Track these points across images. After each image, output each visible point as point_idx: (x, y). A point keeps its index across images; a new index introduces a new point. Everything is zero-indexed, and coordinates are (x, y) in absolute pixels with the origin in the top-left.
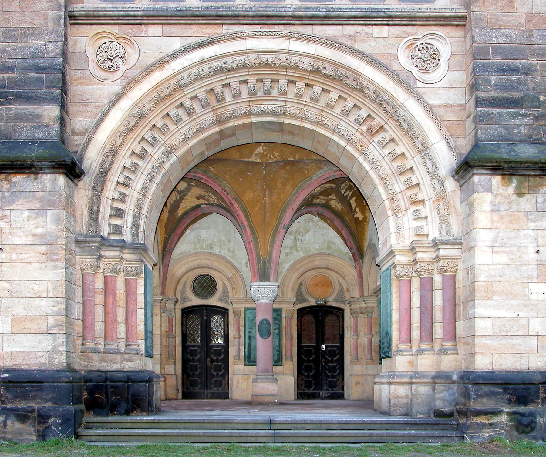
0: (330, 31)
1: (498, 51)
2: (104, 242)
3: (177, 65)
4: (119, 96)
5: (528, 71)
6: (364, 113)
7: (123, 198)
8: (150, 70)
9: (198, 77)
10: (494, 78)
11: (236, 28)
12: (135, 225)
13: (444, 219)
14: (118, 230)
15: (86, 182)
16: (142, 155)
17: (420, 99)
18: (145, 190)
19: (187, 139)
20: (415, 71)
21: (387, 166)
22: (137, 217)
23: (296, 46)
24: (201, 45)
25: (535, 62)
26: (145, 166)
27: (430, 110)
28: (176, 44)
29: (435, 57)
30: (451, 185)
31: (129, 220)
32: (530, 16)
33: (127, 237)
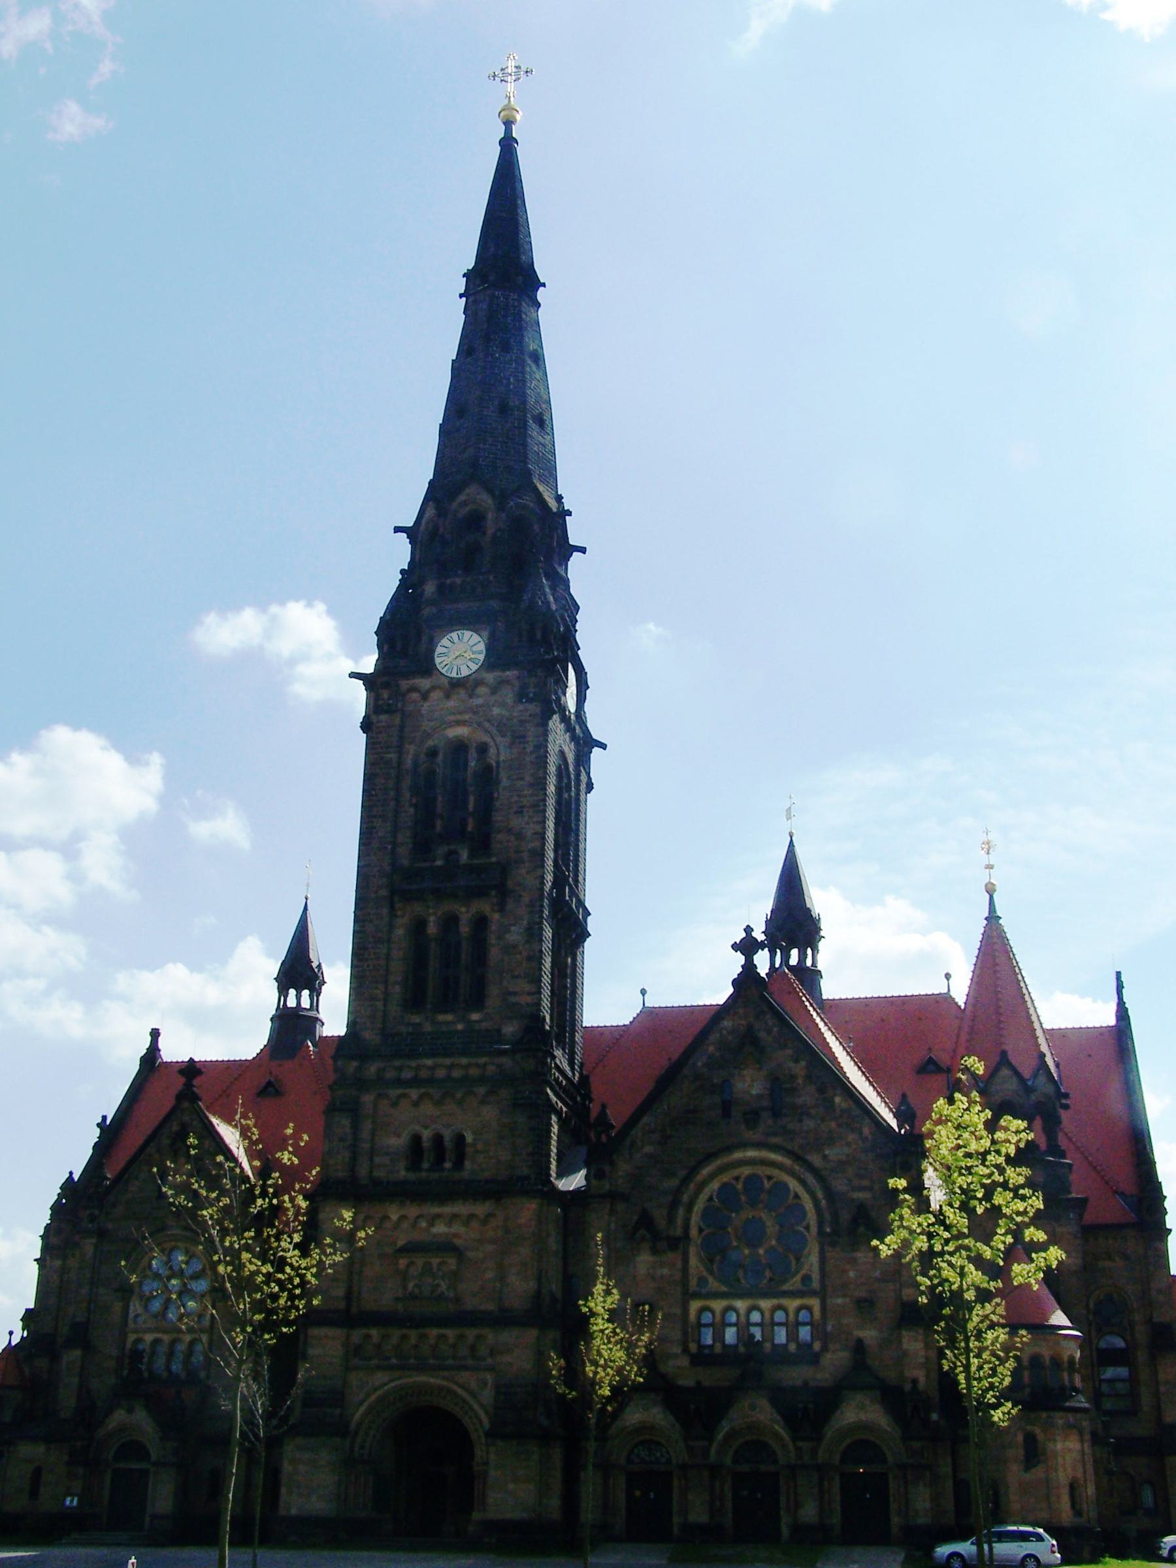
0: (446, 1373)
8: (376, 1389)
23: (432, 1380)
29: (486, 1384)
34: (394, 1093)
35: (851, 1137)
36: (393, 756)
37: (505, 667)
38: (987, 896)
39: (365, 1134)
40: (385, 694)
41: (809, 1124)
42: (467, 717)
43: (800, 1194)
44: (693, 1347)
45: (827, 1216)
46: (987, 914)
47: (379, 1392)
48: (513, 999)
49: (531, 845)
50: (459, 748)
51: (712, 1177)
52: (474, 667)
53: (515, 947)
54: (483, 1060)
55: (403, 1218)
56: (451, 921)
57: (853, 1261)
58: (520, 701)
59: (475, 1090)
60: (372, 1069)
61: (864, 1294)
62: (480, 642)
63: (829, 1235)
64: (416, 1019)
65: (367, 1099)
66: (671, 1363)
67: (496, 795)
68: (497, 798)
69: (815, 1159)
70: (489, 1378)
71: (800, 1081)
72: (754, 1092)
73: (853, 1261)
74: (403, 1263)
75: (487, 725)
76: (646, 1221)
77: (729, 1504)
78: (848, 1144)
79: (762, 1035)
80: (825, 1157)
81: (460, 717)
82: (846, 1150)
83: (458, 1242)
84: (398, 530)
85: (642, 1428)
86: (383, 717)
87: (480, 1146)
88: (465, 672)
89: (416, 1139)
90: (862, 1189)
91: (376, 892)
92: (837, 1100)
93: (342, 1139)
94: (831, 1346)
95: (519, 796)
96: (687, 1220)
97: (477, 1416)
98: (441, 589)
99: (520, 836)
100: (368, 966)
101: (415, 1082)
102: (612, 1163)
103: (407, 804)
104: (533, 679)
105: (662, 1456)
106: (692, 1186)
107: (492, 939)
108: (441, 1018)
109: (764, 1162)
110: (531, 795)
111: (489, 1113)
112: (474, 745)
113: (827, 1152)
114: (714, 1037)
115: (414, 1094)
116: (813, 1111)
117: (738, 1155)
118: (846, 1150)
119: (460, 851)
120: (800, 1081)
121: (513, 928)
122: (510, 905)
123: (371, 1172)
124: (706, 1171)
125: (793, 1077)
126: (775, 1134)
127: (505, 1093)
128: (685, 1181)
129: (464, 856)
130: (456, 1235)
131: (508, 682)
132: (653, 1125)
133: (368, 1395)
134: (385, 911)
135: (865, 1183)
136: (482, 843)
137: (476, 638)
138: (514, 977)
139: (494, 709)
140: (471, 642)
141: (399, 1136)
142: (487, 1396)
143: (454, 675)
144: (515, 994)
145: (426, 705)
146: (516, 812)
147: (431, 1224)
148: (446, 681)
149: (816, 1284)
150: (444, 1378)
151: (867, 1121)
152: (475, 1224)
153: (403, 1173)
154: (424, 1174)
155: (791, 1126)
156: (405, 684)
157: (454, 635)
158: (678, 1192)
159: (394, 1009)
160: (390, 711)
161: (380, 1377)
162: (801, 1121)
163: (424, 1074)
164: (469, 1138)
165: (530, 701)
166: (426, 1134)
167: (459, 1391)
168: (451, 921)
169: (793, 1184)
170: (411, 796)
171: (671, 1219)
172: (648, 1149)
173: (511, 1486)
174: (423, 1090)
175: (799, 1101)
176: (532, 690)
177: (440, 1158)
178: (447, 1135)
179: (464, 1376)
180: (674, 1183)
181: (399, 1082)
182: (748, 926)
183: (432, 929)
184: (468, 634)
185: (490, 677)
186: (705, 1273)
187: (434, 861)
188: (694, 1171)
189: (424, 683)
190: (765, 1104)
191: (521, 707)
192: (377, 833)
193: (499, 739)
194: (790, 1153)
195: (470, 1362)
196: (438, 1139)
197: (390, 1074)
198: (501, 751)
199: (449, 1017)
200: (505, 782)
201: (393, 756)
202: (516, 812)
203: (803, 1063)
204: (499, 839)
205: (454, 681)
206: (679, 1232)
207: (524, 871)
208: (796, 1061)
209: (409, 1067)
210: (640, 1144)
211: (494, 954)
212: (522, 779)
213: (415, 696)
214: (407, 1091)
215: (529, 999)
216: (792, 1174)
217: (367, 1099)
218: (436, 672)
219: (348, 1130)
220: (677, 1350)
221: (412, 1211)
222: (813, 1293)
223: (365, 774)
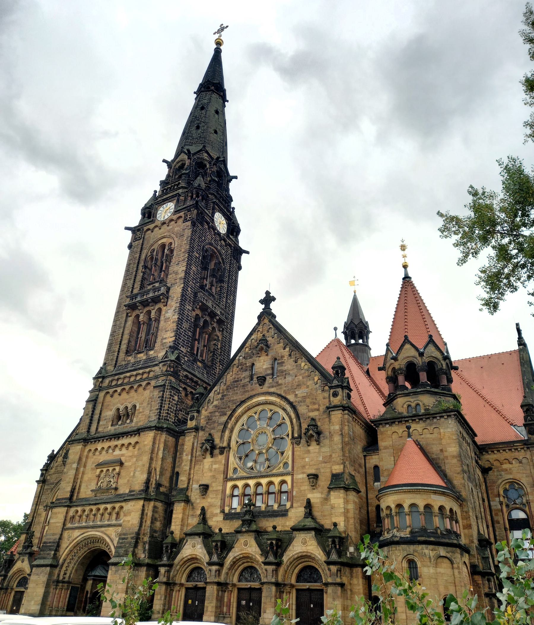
0: (103, 529)
7: (67, 570)
9: (81, 541)
11: (87, 530)
14: (64, 578)
16: (72, 559)
18: (73, 567)
24: (82, 534)
28: (79, 534)
32: (132, 524)
35: (310, 383)
41: (289, 379)
43: (285, 418)
44: (227, 510)
45: (296, 428)
55: (103, 448)
57: (309, 452)
61: (313, 471)
66: (215, 519)
69: (291, 398)
71: (286, 358)
72: (264, 367)
73: (309, 452)
76: (210, 440)
78: (308, 387)
79: (269, 339)
80: (296, 395)
82: (306, 390)
90: (313, 410)
92: (303, 364)
94: (294, 505)
106: (233, 419)
113: (297, 393)
115: (119, 389)
116: (291, 372)
117: (255, 400)
118: (306, 390)
120: (286, 358)
124: (240, 410)
125: (282, 357)
126: (273, 387)
135: (316, 406)
141: (111, 410)
144: (166, 338)
147: (114, 450)
150: (102, 532)
151: (317, 373)
152: (131, 448)
153: (110, 427)
155: (280, 382)
161: (77, 533)
162: (285, 378)
166: (121, 408)
169: (281, 412)
171: (222, 437)
172: (215, 403)
175: (285, 368)
188: (234, 411)
194: (280, 396)
203: (287, 349)
206: (225, 444)
208: (284, 349)
209: (120, 378)
220: (218, 511)
222: (287, 474)
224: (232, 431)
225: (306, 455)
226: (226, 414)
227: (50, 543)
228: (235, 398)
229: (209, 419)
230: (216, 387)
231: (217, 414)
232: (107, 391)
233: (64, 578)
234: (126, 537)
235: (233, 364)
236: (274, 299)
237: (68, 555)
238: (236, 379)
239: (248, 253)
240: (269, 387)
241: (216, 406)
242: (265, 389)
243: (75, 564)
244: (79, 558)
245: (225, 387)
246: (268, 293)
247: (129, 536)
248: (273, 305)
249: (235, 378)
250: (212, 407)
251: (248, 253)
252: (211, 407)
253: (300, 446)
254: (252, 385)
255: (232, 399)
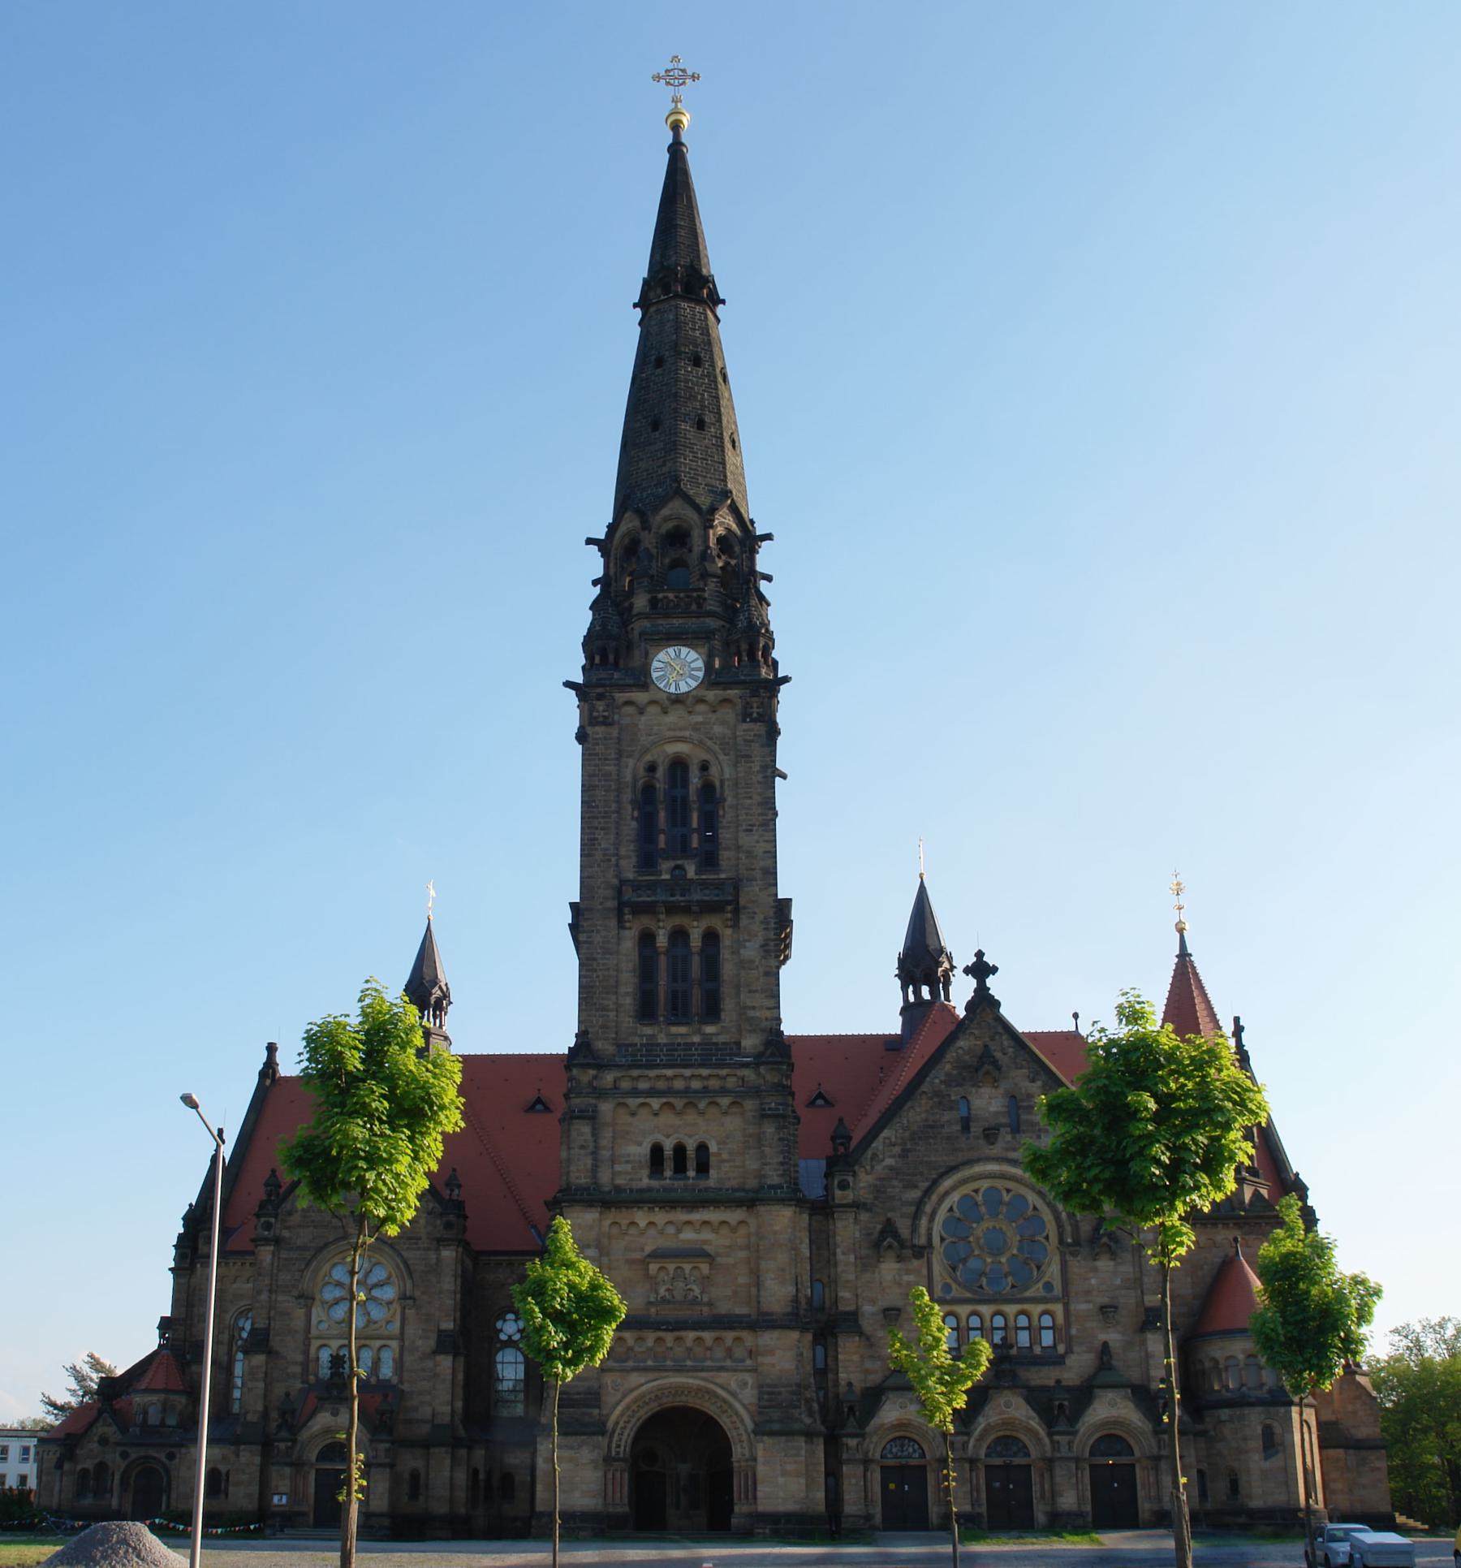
0: (704, 1374)
1: (769, 1386)
2: (615, 1460)
3: (644, 1388)
4: (621, 1401)
5: (779, 1393)
6: (719, 1405)
7: (620, 1440)
8: (633, 1390)
9: (652, 1392)
10: (766, 1397)
12: (625, 1450)
13: (751, 1450)
14: (618, 1453)
15: (608, 1434)
17: (740, 1401)
18: (629, 1435)
19: (646, 1413)
20: (738, 1391)
21: (730, 1425)
22: (625, 1447)
23: (691, 1381)
25: (782, 1389)
26: (630, 1426)
27: (744, 1405)
28: (643, 1380)
30: (752, 1436)
31: (622, 1448)
33: (622, 1455)
34: (633, 1102)
36: (612, 769)
37: (726, 685)
38: (1178, 935)
39: (604, 1142)
40: (600, 706)
42: (687, 734)
43: (1038, 1206)
45: (1068, 1229)
46: (1178, 953)
47: (636, 1393)
48: (751, 1013)
49: (762, 864)
50: (679, 765)
51: (954, 1188)
52: (694, 684)
53: (752, 962)
54: (724, 1072)
55: (651, 1223)
56: (679, 936)
58: (744, 721)
59: (719, 1100)
60: (609, 1078)
62: (698, 659)
63: (1069, 1245)
64: (648, 1030)
65: (606, 1107)
67: (721, 813)
68: (724, 816)
70: (749, 1378)
72: (992, 1109)
74: (653, 1268)
75: (709, 743)
76: (889, 1229)
77: (984, 1495)
79: (998, 1055)
81: (678, 734)
83: (708, 1248)
84: (589, 541)
85: (902, 1425)
86: (600, 729)
87: (725, 1156)
88: (684, 688)
89: (657, 1151)
91: (601, 904)
93: (582, 1147)
95: (747, 814)
96: (930, 1230)
97: (737, 1414)
98: (654, 603)
99: (750, 854)
100: (598, 977)
101: (652, 1093)
102: (854, 1174)
103: (629, 817)
104: (756, 699)
105: (915, 1451)
106: (934, 1197)
107: (725, 954)
108: (674, 1030)
109: (1003, 1176)
110: (759, 815)
111: (733, 1123)
112: (696, 761)
114: (951, 1055)
115: (655, 1103)
117: (978, 1169)
119: (687, 867)
121: (747, 944)
122: (744, 921)
123: (613, 1179)
124: (947, 1183)
127: (750, 1105)
128: (928, 1192)
129: (691, 872)
130: (705, 1242)
131: (726, 701)
132: (893, 1140)
133: (625, 1396)
134: (613, 923)
136: (709, 860)
137: (693, 655)
138: (750, 992)
139: (715, 727)
140: (689, 659)
141: (640, 1144)
142: (749, 1395)
143: (672, 690)
144: (754, 1008)
145: (643, 718)
146: (747, 830)
147: (679, 1231)
148: (665, 695)
149: (1058, 1290)
150: (704, 1379)
154: (668, 1181)
156: (621, 697)
157: (671, 650)
158: (920, 1204)
159: (628, 1021)
160: (606, 722)
161: (635, 1379)
162: (1039, 1137)
163: (661, 1085)
164: (713, 1148)
165: (753, 720)
166: (668, 1146)
167: (720, 1392)
168: (679, 936)
170: (633, 810)
171: (914, 1229)
172: (889, 1161)
173: (781, 1480)
174: (664, 1100)
176: (755, 710)
177: (680, 1167)
178: (691, 1146)
179: (723, 1377)
180: (915, 1194)
181: (635, 1093)
182: (980, 951)
183: (662, 940)
184: (684, 650)
185: (711, 695)
186: (949, 1280)
187: (661, 875)
188: (935, 1183)
189: (640, 697)
190: (1004, 1120)
191: (745, 726)
192: (600, 844)
193: (722, 757)
195: (728, 1363)
196: (680, 1149)
197: (625, 1085)
198: (723, 770)
199: (682, 1030)
200: (730, 801)
201: (612, 769)
202: (747, 830)
204: (726, 856)
205: (673, 697)
206: (923, 1241)
207: (757, 889)
210: (881, 1156)
211: (728, 969)
212: (750, 798)
213: (629, 709)
214: (648, 1100)
215: (768, 1014)
216: (1033, 1188)
217: (606, 1107)
218: (652, 686)
219: (589, 1137)
221: (660, 1217)
222: (1055, 1300)
223: (582, 786)
224: (932, 1219)
225: (1091, 1275)
226: (916, 1187)
227: (578, 1393)
228: (933, 1159)
229: (878, 1190)
230: (886, 1131)
231: (895, 1183)
232: (621, 1100)
233: (618, 1453)
234: (776, 1390)
235: (920, 1091)
236: (994, 970)
237: (622, 1414)
238: (931, 1123)
239: (784, 777)
240: (1007, 1150)
241: (891, 1168)
242: (996, 1150)
243: (631, 1430)
244: (638, 1420)
245: (907, 1134)
246: (980, 954)
247: (782, 1389)
248: (991, 981)
249: (927, 1120)
250: (884, 1168)
251: (784, 777)
252: (879, 1168)
253: (1079, 1258)
254: (968, 1138)
255: (925, 1159)
